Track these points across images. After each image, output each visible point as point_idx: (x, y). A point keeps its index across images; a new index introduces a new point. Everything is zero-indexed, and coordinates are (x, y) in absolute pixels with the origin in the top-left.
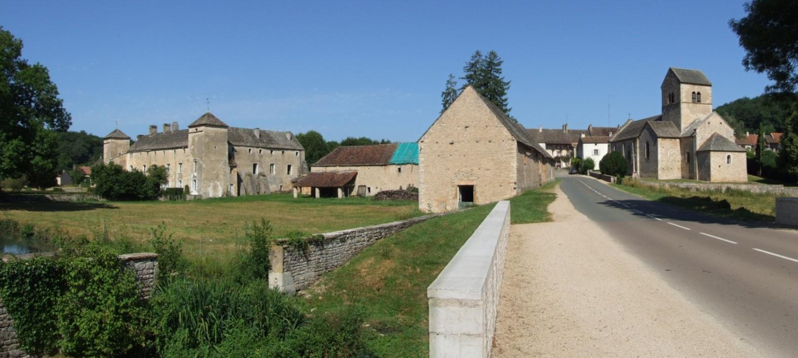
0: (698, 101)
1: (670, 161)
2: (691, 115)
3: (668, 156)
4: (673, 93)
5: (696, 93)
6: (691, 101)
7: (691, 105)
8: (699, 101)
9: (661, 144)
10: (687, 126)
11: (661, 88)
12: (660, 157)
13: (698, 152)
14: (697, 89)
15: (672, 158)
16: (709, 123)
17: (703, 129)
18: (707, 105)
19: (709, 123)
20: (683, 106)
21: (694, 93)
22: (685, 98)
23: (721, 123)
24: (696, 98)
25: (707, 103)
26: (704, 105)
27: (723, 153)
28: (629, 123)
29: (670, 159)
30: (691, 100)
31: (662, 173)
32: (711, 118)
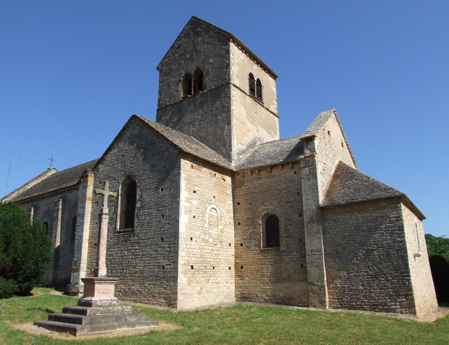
1: (211, 240)
3: (206, 225)
5: (256, 79)
9: (189, 181)
10: (244, 147)
12: (184, 220)
13: (322, 210)
15: (214, 232)
16: (329, 132)
20: (235, 93)
21: (251, 76)
22: (237, 76)
24: (255, 90)
26: (268, 112)
28: (50, 174)
30: (247, 89)
31: (190, 282)
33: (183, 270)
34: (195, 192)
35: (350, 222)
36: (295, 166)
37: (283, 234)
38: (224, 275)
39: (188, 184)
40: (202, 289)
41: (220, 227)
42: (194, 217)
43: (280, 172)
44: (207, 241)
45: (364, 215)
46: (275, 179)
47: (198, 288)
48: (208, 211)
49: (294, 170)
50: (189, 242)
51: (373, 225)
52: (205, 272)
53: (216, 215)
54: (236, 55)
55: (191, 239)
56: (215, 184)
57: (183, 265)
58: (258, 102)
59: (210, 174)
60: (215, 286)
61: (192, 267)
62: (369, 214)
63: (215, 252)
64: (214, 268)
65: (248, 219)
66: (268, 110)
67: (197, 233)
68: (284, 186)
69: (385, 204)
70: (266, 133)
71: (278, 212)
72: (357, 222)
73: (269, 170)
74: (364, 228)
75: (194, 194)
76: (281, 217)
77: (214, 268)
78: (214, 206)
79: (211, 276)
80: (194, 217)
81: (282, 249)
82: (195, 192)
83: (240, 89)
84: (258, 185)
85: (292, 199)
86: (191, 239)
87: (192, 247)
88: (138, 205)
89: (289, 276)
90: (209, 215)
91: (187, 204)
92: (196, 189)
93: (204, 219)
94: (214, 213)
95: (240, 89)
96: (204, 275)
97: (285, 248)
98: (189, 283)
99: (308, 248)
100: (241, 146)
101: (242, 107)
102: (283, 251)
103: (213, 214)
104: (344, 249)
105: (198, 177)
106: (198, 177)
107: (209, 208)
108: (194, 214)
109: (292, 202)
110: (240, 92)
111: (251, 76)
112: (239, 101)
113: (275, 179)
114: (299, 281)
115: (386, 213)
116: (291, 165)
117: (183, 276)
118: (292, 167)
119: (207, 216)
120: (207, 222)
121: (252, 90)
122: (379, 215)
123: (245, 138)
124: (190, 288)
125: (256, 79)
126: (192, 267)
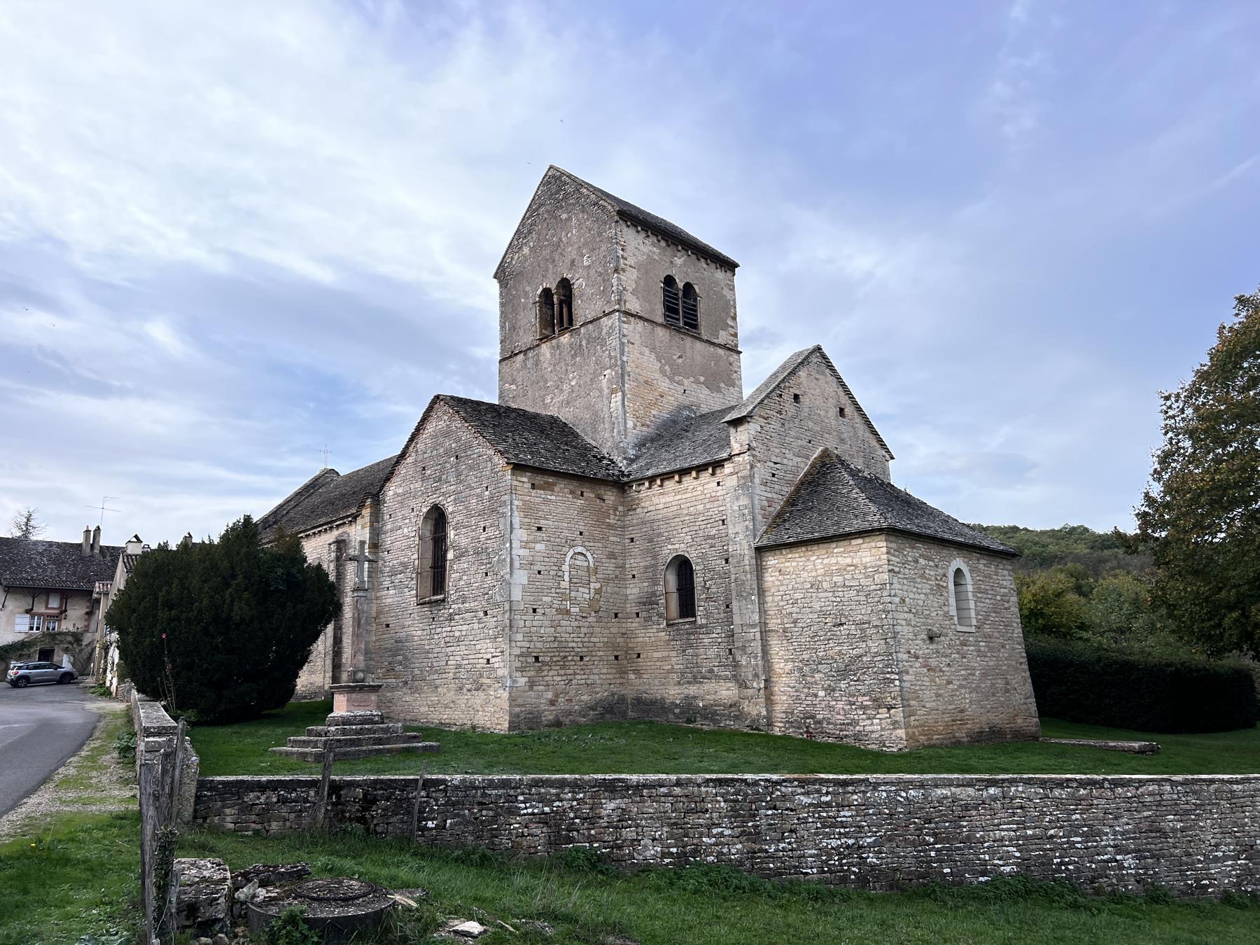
0: (686, 323)
1: (575, 610)
2: (664, 384)
3: (565, 584)
4: (565, 285)
6: (660, 319)
7: (660, 332)
8: (691, 325)
11: (502, 275)
14: (682, 268)
15: (584, 594)
16: (796, 397)
17: (775, 424)
18: (721, 352)
19: (796, 397)
21: (669, 281)
23: (842, 410)
25: (720, 341)
26: (712, 349)
27: (933, 552)
29: (574, 601)
30: (659, 314)
31: (532, 684)
32: (802, 373)
33: (519, 665)
34: (539, 529)
35: (805, 575)
36: (718, 471)
37: (699, 595)
38: (605, 671)
39: (526, 517)
40: (557, 696)
41: (592, 585)
42: (539, 572)
43: (696, 482)
44: (568, 612)
45: (826, 561)
46: (688, 495)
47: (550, 695)
48: (568, 559)
49: (716, 479)
50: (530, 616)
51: (840, 579)
52: (563, 667)
53: (586, 564)
54: (630, 248)
55: (534, 610)
56: (582, 510)
57: (522, 655)
58: (685, 334)
59: (572, 492)
60: (584, 690)
61: (537, 658)
62: (833, 561)
63: (584, 630)
64: (582, 658)
65: (646, 567)
66: (714, 344)
67: (545, 599)
68: (700, 507)
69: (860, 541)
70: (707, 392)
71: (692, 556)
72: (814, 574)
73: (677, 478)
74: (825, 585)
75: (538, 534)
76: (697, 564)
77: (582, 658)
78: (580, 549)
79: (575, 674)
80: (539, 572)
81: (700, 621)
82: (539, 529)
83: (640, 318)
84: (661, 506)
85: (714, 532)
86: (534, 610)
87: (535, 623)
88: (450, 555)
89: (711, 671)
90: (570, 566)
91: (523, 552)
92: (542, 523)
93: (560, 573)
94: (580, 562)
95: (640, 318)
96: (562, 672)
97: (704, 621)
98: (531, 688)
99: (737, 620)
100: (644, 429)
101: (647, 352)
102: (701, 626)
103: (578, 563)
104: (795, 622)
105: (546, 501)
106: (546, 501)
107: (570, 554)
108: (537, 568)
109: (713, 537)
110: (641, 323)
111: (669, 281)
112: (637, 343)
113: (688, 495)
114: (726, 679)
115: (861, 557)
116: (710, 470)
117: (519, 674)
118: (713, 474)
119: (566, 568)
120: (567, 578)
121: (670, 310)
122: (849, 561)
123: (654, 412)
124: (532, 693)
125: (681, 285)
126: (537, 658)
